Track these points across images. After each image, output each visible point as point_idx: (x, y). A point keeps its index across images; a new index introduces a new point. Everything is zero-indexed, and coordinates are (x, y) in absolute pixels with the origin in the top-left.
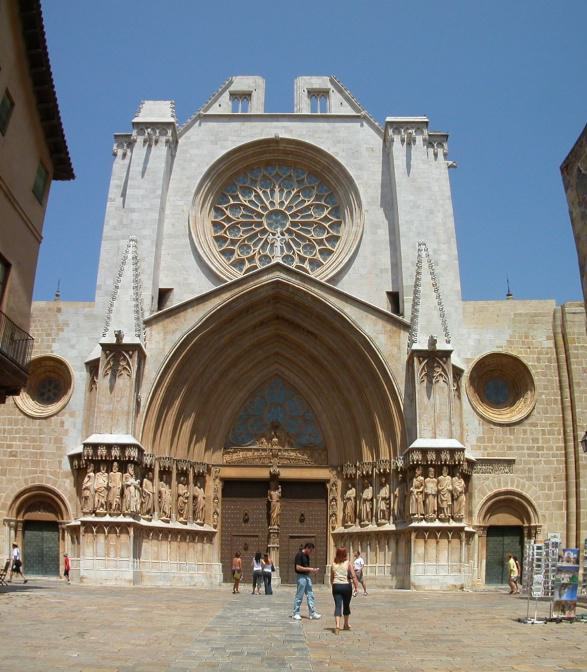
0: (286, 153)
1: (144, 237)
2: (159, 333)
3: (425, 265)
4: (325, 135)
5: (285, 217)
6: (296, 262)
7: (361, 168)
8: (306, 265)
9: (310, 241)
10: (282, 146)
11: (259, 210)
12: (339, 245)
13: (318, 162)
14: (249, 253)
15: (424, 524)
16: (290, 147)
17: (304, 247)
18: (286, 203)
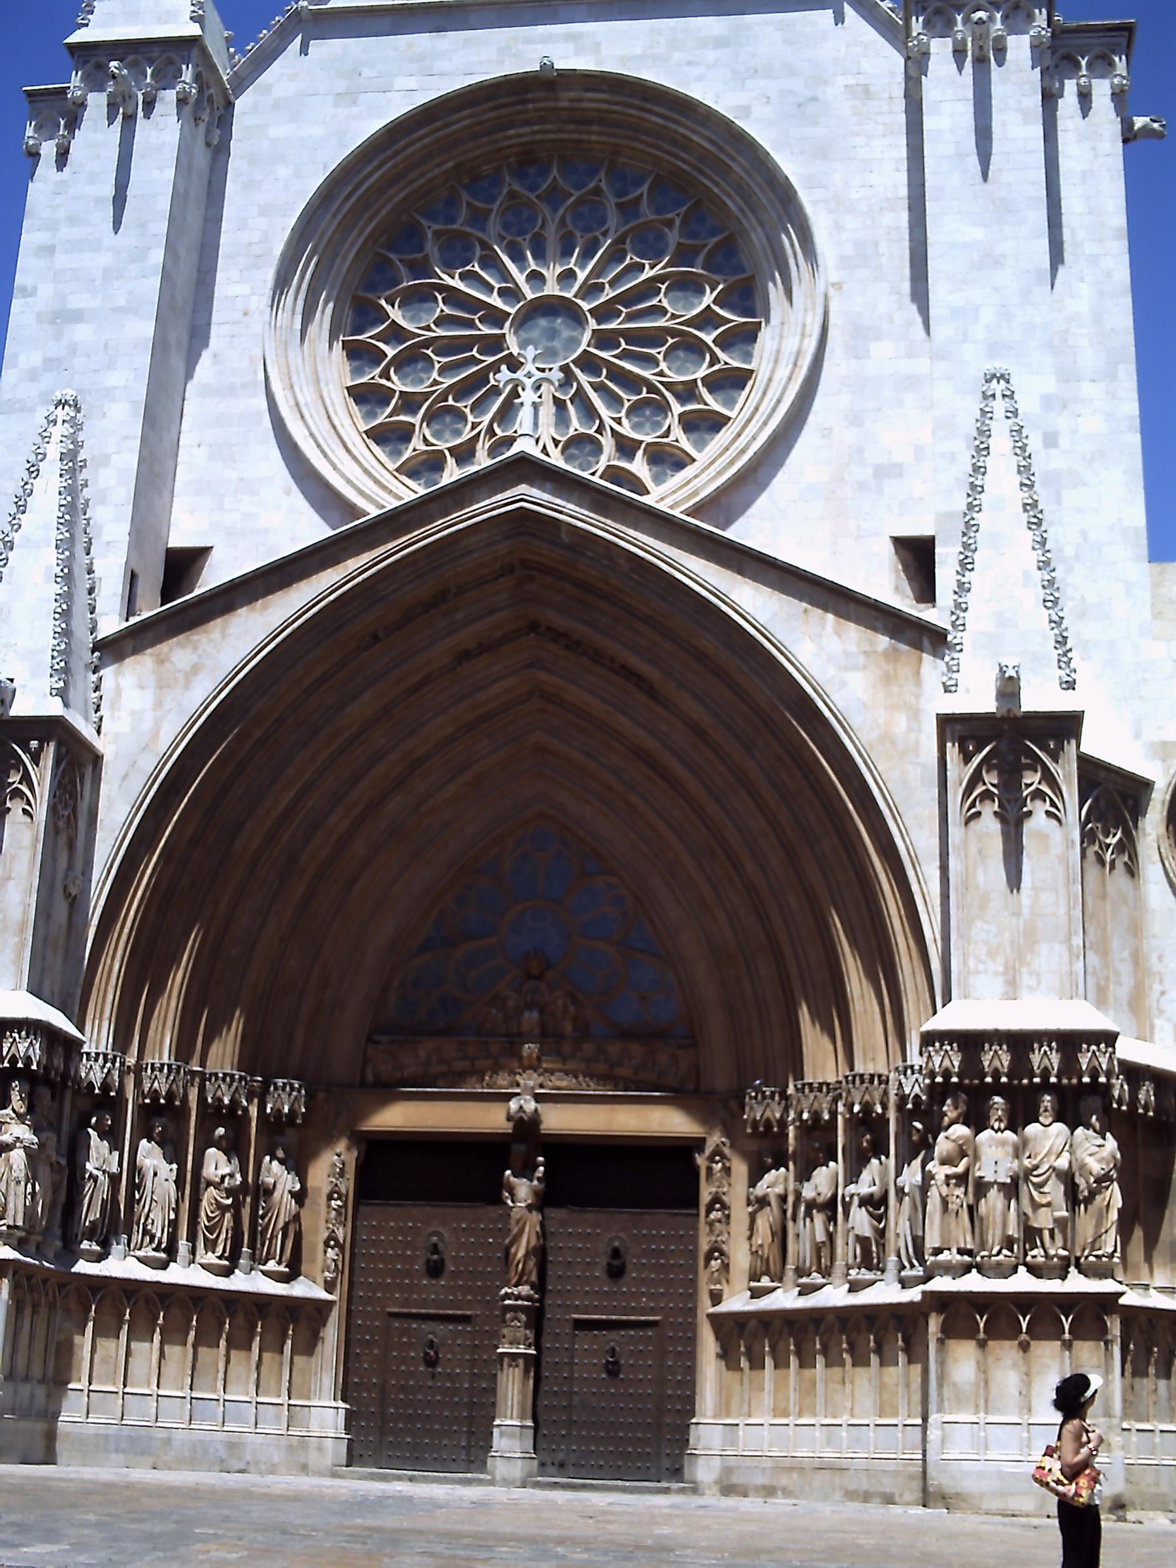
0: (583, 120)
1: (109, 394)
2: (142, 688)
3: (1001, 441)
4: (711, 55)
5: (576, 317)
6: (608, 455)
7: (822, 152)
8: (639, 466)
9: (652, 388)
10: (565, 98)
11: (495, 300)
12: (747, 398)
13: (685, 144)
14: (458, 433)
15: (974, 1283)
16: (593, 101)
17: (634, 409)
18: (582, 275)
